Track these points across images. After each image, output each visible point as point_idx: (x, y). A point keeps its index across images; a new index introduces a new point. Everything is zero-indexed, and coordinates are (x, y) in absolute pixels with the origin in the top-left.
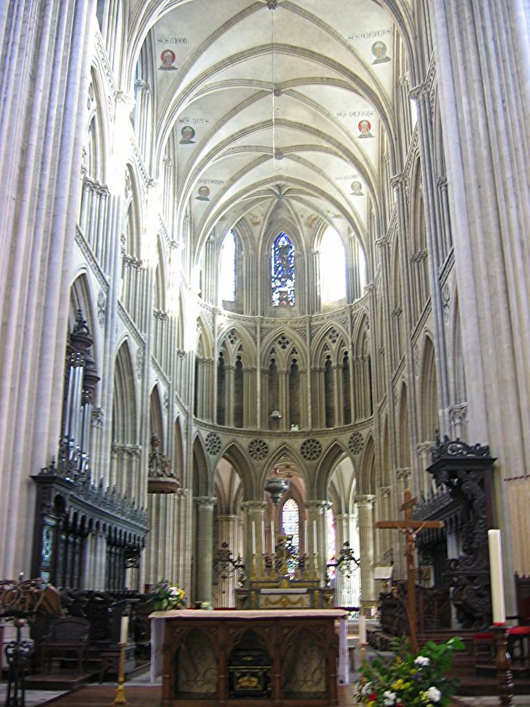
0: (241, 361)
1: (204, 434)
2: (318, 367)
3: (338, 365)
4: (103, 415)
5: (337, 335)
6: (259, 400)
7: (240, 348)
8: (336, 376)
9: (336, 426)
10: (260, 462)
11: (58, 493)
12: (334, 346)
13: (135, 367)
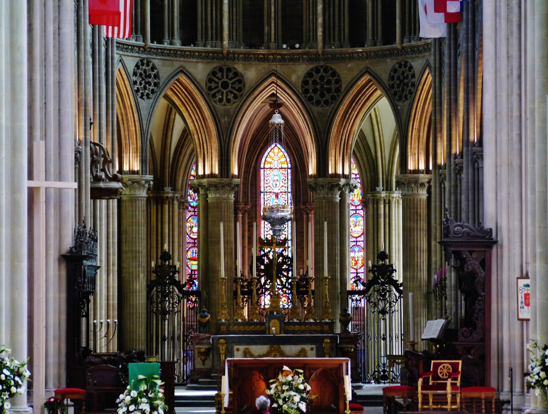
1: (131, 63)
10: (229, 106)
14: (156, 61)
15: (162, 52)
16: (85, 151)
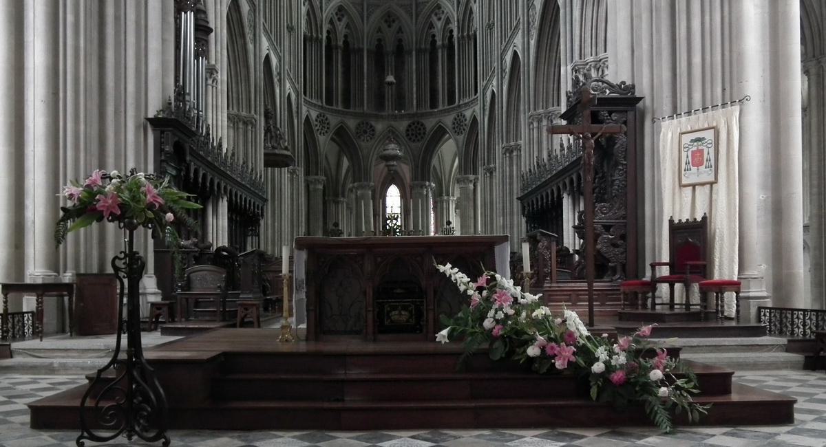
0: (349, 40)
1: (314, 114)
2: (423, 46)
3: (443, 44)
4: (217, 72)
5: (443, 12)
6: (365, 81)
7: (348, 26)
8: (441, 55)
9: (441, 108)
11: (176, 139)
13: (247, 30)
14: (328, 116)
15: (332, 111)
16: (260, 120)
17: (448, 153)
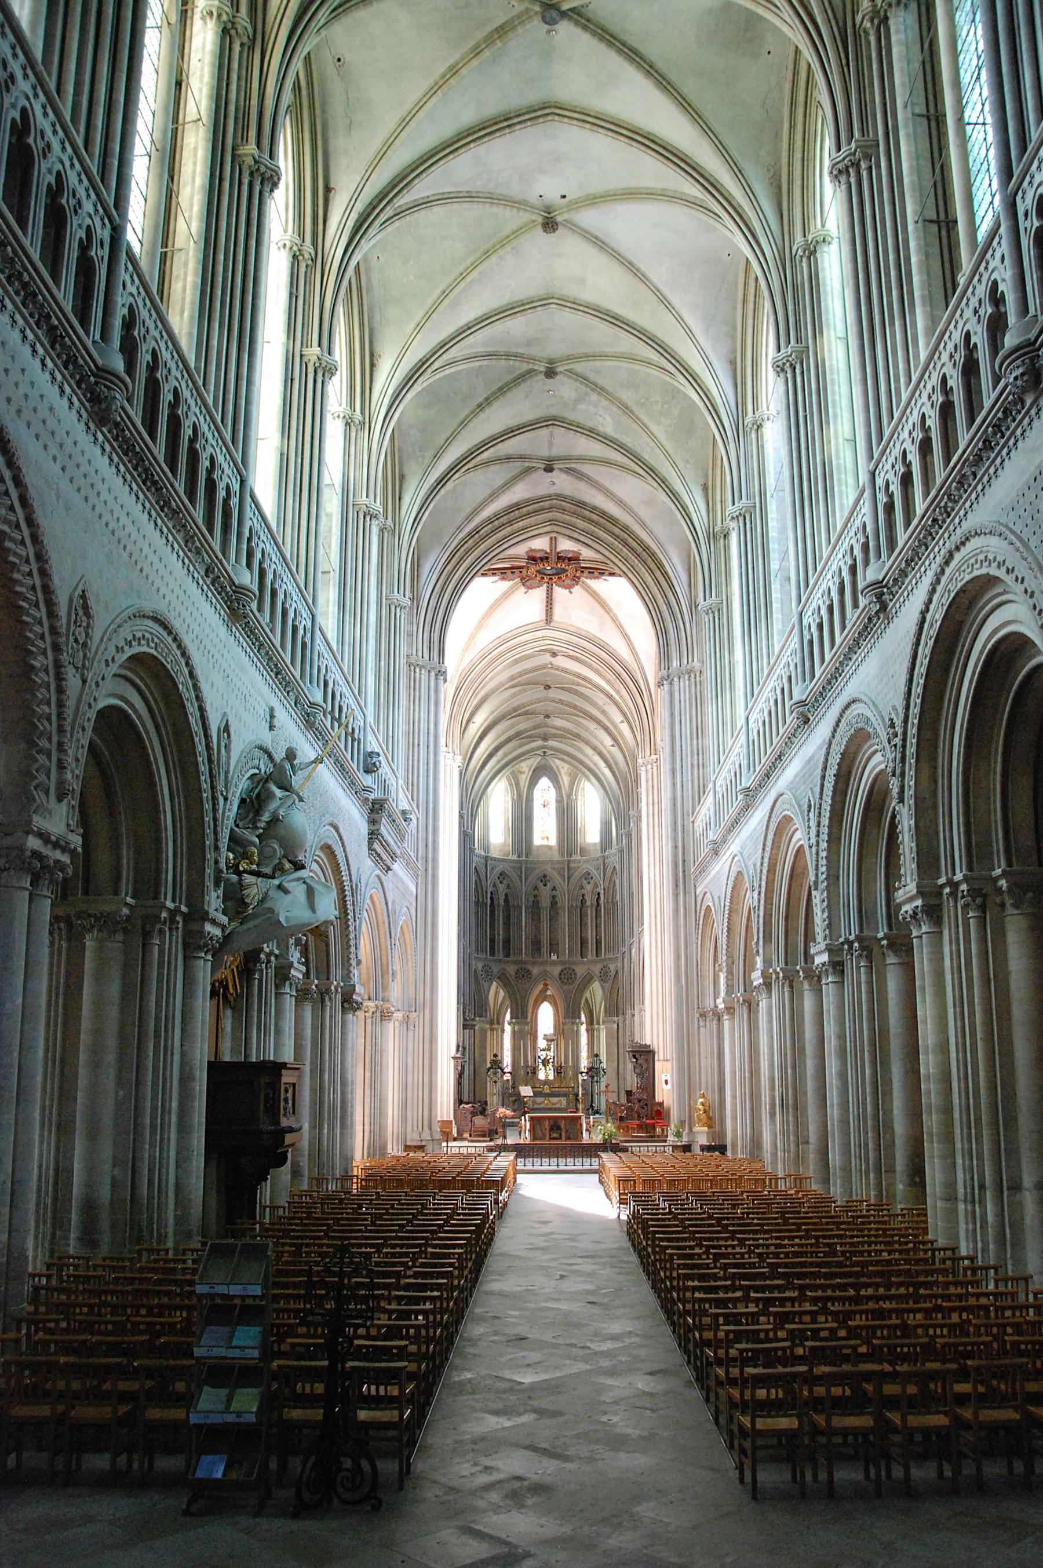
1: (480, 966)
7: (508, 886)
12: (589, 888)
14: (492, 965)
17: (596, 992)
